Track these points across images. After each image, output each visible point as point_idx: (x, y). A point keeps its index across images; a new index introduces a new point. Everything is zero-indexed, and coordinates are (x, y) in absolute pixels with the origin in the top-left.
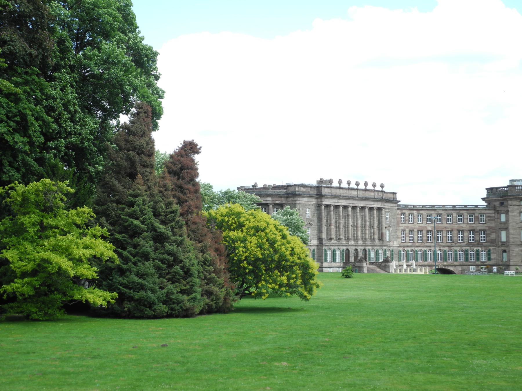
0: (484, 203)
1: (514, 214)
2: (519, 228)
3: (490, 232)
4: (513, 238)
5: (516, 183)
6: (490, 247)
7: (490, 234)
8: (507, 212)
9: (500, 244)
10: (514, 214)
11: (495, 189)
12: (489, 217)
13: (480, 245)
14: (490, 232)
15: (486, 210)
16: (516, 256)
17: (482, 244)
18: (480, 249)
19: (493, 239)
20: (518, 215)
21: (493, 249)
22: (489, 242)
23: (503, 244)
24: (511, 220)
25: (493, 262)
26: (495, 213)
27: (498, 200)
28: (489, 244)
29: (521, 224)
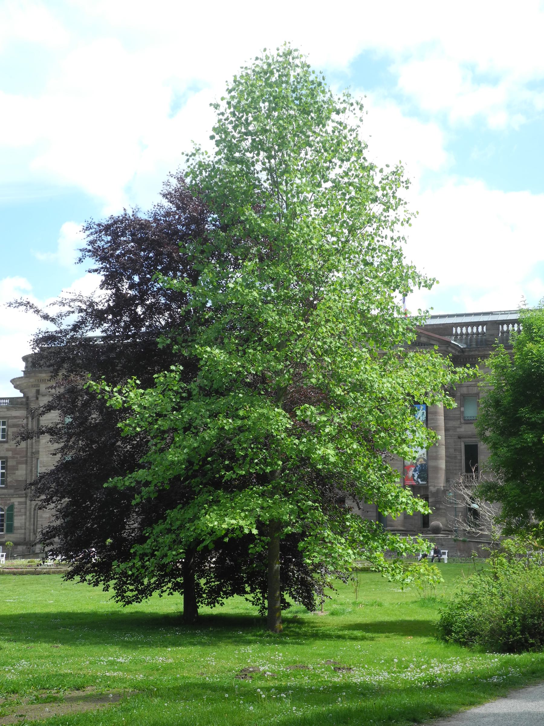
0: (17, 394)
3: (15, 463)
6: (13, 500)
7: (15, 468)
12: (14, 426)
14: (15, 463)
15: (8, 408)
19: (20, 479)
21: (20, 503)
22: (11, 487)
25: (18, 536)
26: (27, 418)
28: (12, 491)
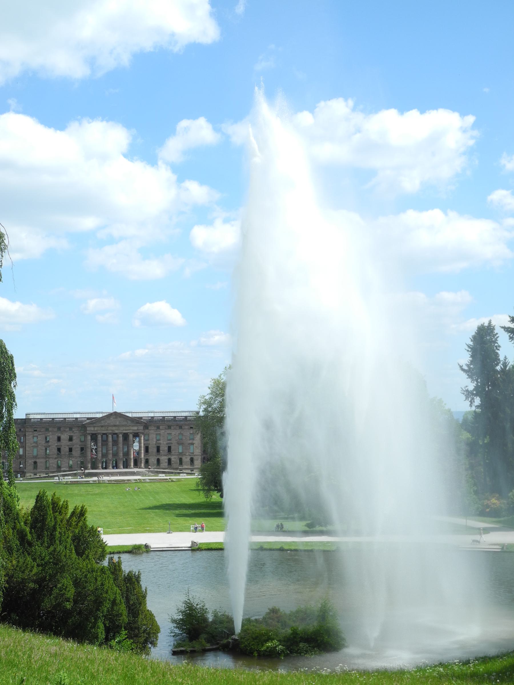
1: (29, 437)
2: (32, 447)
4: (28, 453)
5: (31, 417)
8: (25, 436)
9: (18, 457)
10: (29, 437)
11: (16, 420)
13: (5, 458)
16: (29, 465)
17: (6, 458)
18: (5, 461)
20: (32, 438)
23: (21, 457)
24: (27, 442)
27: (19, 428)
29: (33, 444)
